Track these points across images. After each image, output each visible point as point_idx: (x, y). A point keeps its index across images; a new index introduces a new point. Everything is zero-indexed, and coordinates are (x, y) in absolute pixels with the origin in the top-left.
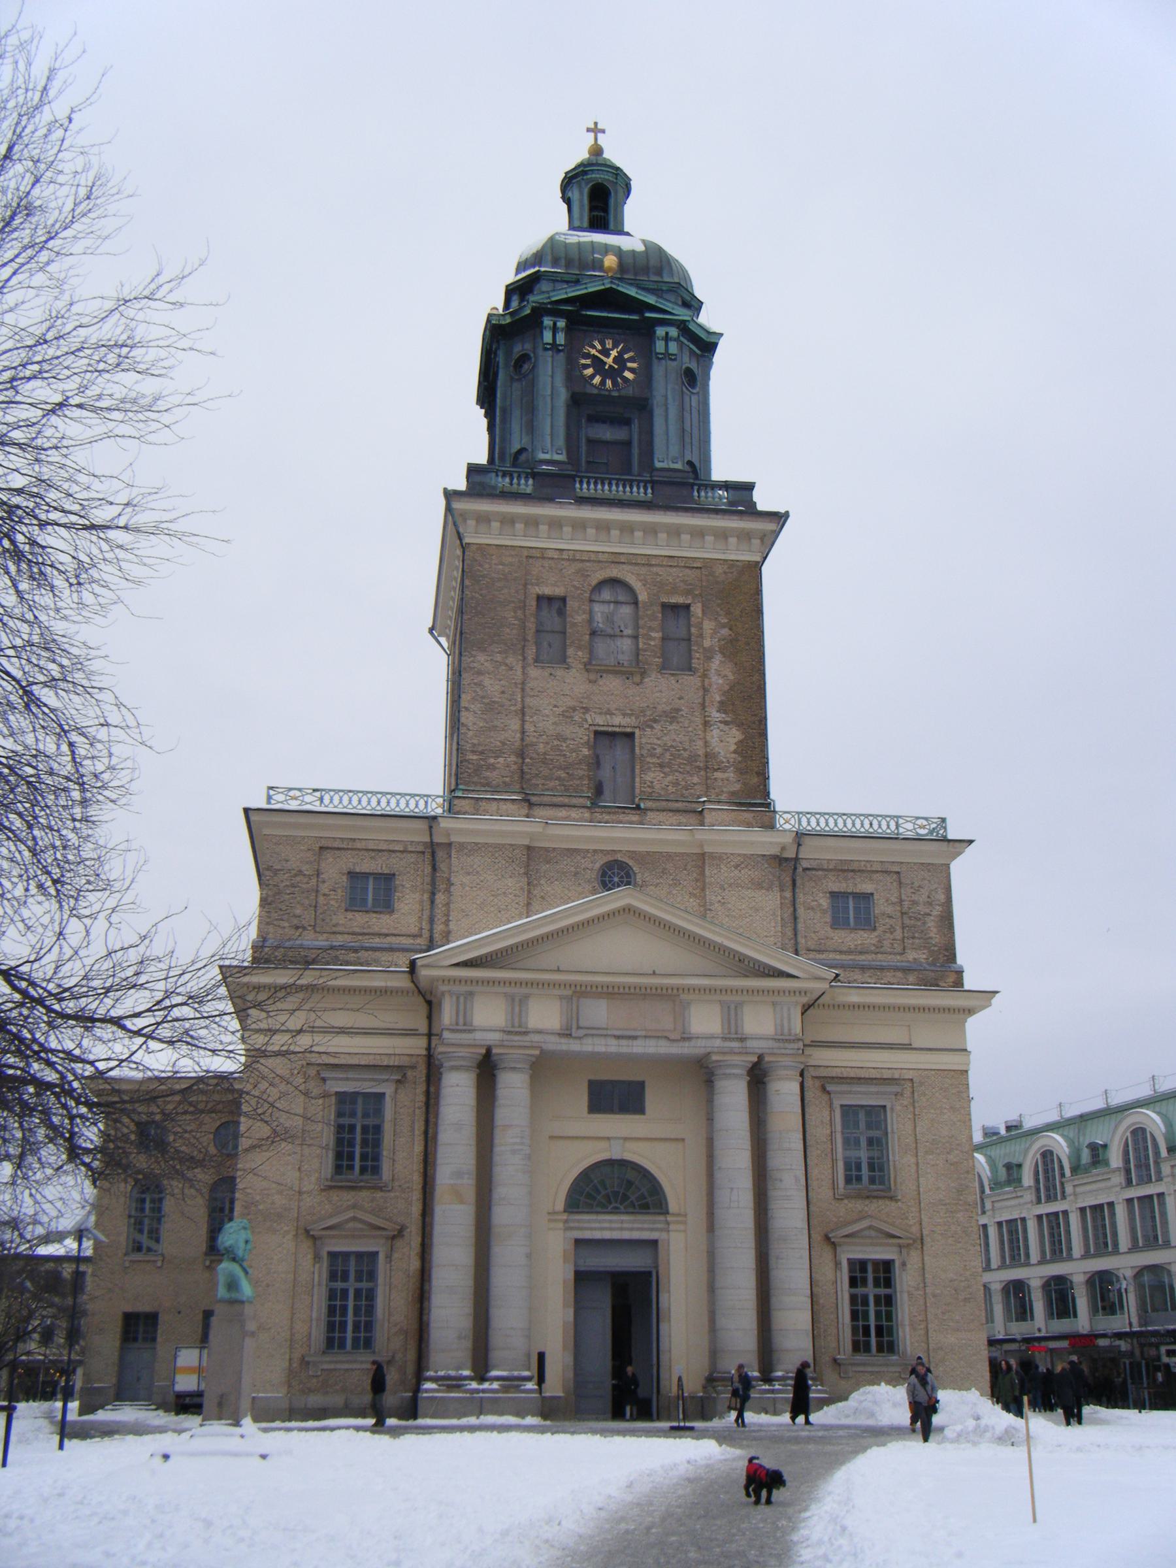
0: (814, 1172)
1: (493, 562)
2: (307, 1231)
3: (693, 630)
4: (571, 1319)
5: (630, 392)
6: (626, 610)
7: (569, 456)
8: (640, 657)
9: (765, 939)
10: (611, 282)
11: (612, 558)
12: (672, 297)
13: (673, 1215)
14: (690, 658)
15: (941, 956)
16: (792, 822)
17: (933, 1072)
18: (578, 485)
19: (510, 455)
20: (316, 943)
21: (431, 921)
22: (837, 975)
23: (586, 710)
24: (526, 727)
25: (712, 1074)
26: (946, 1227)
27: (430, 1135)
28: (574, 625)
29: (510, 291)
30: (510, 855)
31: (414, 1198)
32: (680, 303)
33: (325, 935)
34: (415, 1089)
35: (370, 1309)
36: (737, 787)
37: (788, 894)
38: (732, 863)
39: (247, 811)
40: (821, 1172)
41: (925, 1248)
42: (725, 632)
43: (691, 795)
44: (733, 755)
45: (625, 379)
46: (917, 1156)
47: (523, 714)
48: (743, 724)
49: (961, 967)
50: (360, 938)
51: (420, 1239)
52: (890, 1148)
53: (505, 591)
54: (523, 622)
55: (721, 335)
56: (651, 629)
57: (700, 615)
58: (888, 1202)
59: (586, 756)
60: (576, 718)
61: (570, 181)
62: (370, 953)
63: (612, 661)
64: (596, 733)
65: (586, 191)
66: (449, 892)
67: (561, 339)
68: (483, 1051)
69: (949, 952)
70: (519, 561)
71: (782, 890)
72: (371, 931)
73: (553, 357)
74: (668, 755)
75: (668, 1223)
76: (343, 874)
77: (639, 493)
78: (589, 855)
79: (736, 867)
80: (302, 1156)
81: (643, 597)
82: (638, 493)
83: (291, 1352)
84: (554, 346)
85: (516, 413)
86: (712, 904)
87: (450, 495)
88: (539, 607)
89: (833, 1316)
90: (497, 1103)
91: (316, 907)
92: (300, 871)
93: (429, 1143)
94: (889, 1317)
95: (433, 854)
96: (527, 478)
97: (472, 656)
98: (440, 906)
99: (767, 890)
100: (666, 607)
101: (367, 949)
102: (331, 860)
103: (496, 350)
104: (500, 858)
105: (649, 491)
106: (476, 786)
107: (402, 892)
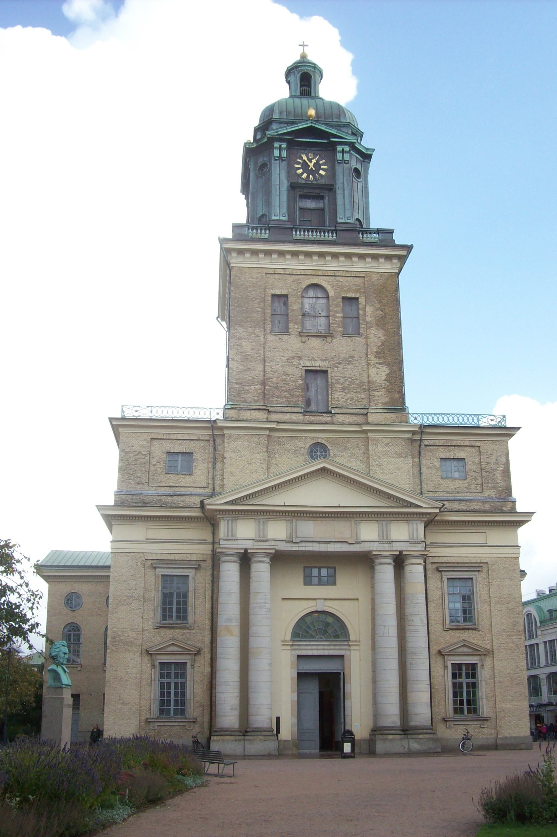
0: (432, 616)
1: (247, 277)
2: (147, 651)
3: (360, 312)
4: (296, 699)
5: (323, 181)
6: (322, 302)
7: (289, 216)
8: (331, 328)
9: (404, 485)
10: (312, 123)
11: (313, 273)
12: (345, 130)
13: (353, 641)
14: (359, 328)
15: (503, 493)
16: (418, 419)
17: (500, 558)
18: (294, 233)
19: (257, 218)
20: (149, 492)
21: (214, 478)
22: (444, 505)
23: (300, 358)
24: (266, 368)
25: (374, 562)
26: (506, 645)
27: (215, 599)
28: (293, 311)
29: (256, 130)
30: (258, 441)
31: (206, 633)
32: (350, 133)
33: (154, 488)
34: (206, 573)
35: (183, 694)
36: (387, 400)
37: (416, 460)
38: (384, 443)
39: (111, 420)
40: (435, 616)
41: (494, 656)
42: (379, 313)
43: (361, 405)
44: (384, 382)
45: (320, 175)
46: (490, 606)
47: (265, 362)
48: (389, 364)
49: (515, 499)
50: (174, 488)
51: (210, 656)
52: (475, 601)
53: (254, 292)
54: (264, 309)
55: (374, 150)
56: (336, 312)
57: (364, 303)
58: (474, 631)
59: (300, 384)
60: (295, 363)
61: (289, 72)
62: (179, 497)
63: (314, 331)
64: (306, 371)
65: (298, 76)
66: (224, 462)
67: (284, 154)
68: (243, 551)
69: (508, 490)
70: (261, 276)
71: (413, 458)
72: (181, 485)
73: (280, 164)
74: (347, 383)
75: (349, 645)
76: (164, 453)
77: (329, 237)
78: (303, 440)
79: (387, 445)
80: (144, 610)
81: (331, 294)
82: (328, 236)
83: (140, 716)
84: (280, 158)
85: (260, 195)
86: (373, 466)
87: (222, 241)
88: (273, 301)
89: (442, 695)
90: (251, 580)
91: (149, 472)
92: (140, 452)
93: (214, 603)
94: (474, 694)
95: (214, 440)
96: (265, 230)
97: (237, 330)
98: (219, 470)
99: (405, 458)
100: (344, 298)
101: (178, 495)
102: (157, 446)
103: (249, 162)
104: (252, 443)
105: (335, 235)
106: (238, 402)
107: (197, 463)
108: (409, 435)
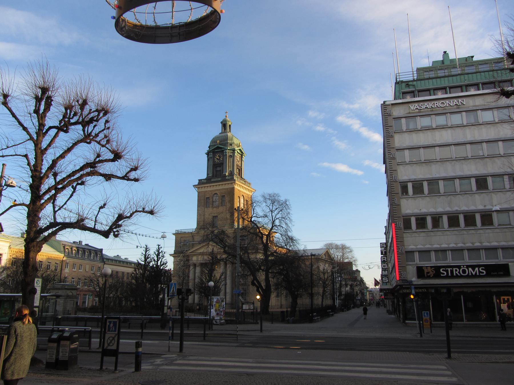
6: (217, 197)
29: (209, 147)
61: (222, 123)
63: (215, 206)
64: (213, 217)
67: (212, 156)
77: (219, 179)
88: (207, 199)
100: (222, 196)
108: (233, 231)
